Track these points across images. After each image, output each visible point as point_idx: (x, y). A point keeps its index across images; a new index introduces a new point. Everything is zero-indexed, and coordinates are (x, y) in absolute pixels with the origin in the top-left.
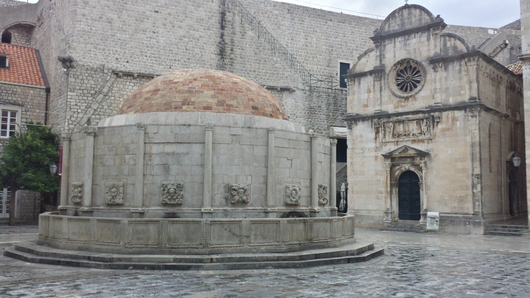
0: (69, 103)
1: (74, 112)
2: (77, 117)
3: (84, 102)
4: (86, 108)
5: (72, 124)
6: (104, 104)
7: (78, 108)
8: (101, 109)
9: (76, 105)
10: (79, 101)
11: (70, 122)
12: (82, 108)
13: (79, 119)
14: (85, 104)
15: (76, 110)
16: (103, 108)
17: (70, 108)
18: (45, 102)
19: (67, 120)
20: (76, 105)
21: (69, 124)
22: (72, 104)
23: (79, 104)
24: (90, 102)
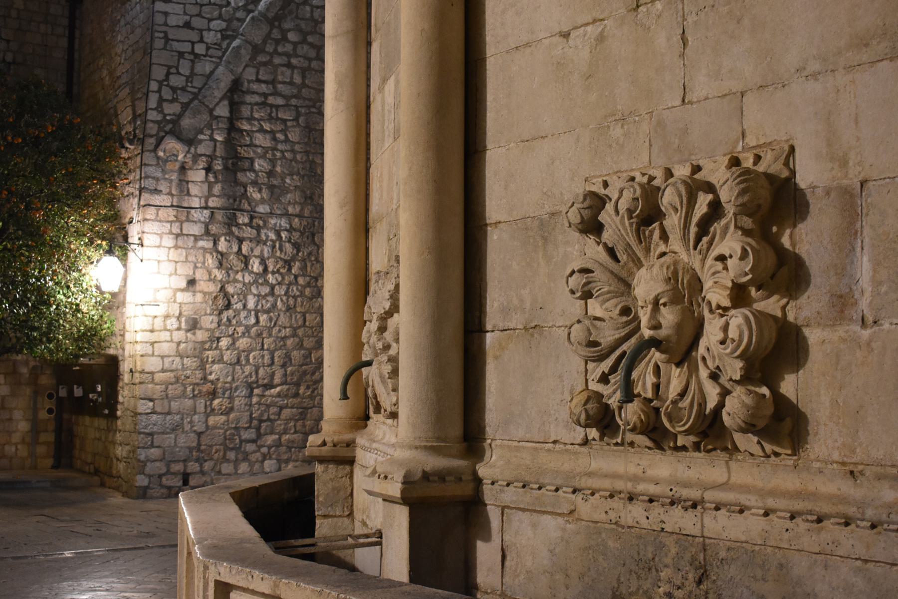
0: (159, 19)
1: (181, 55)
2: (193, 74)
3: (216, 13)
4: (224, 38)
5: (174, 100)
6: (287, 25)
7: (194, 36)
8: (277, 42)
9: (187, 25)
10: (194, 10)
11: (167, 94)
12: (210, 37)
13: (198, 82)
14: (224, 25)
15: (187, 47)
16: (285, 39)
17: (167, 39)
18: (64, 42)
19: (154, 86)
20: (187, 25)
21: (161, 100)
22: (172, 21)
23: (197, 22)
24: (239, 14)
